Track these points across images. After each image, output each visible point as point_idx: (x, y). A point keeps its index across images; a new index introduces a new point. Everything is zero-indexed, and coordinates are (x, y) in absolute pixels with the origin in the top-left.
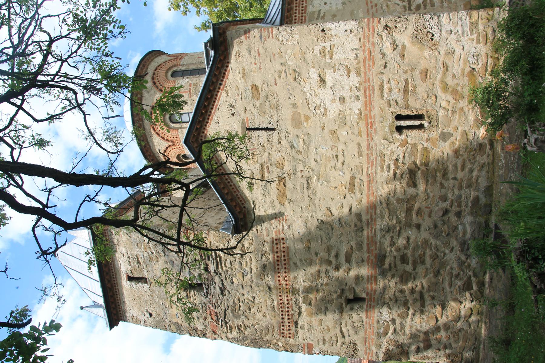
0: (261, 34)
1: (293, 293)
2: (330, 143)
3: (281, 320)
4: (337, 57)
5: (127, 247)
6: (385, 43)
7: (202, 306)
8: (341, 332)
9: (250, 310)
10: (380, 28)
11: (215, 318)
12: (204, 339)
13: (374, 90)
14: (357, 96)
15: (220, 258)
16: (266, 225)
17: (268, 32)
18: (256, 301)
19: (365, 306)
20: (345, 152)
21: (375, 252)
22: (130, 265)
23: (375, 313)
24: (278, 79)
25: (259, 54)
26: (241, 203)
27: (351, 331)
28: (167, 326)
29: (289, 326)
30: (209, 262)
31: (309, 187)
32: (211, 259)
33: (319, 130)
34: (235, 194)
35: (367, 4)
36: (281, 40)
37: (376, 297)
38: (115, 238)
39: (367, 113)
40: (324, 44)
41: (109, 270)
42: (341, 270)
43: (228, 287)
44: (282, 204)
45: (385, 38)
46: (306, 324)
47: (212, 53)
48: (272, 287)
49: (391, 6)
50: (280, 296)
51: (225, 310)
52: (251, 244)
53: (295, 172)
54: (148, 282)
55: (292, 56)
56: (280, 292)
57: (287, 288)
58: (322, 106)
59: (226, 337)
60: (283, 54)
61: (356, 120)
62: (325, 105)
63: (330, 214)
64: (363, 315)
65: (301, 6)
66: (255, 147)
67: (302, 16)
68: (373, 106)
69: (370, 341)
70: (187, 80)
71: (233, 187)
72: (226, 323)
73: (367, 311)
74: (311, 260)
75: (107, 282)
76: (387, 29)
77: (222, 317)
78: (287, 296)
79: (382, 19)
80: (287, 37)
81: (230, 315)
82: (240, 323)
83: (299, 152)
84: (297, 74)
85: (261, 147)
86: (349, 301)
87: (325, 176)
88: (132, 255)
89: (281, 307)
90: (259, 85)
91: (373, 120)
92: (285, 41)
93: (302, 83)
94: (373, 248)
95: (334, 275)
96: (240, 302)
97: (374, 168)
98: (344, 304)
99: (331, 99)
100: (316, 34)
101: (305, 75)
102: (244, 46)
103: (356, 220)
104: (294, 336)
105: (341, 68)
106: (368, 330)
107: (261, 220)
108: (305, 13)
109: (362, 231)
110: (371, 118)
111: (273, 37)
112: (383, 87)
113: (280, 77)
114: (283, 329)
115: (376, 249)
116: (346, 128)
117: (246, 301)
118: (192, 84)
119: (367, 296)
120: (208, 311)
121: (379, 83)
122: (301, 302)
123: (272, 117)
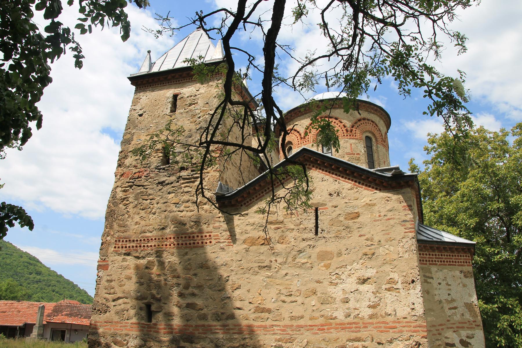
0: (408, 221)
1: (157, 252)
2: (303, 289)
3: (132, 239)
4: (387, 296)
5: (205, 94)
6: (402, 343)
7: (148, 164)
8: (119, 298)
9: (143, 210)
10: (418, 339)
11: (136, 175)
12: (116, 165)
13: (356, 332)
14: (349, 316)
15: (193, 182)
16: (225, 226)
17: (410, 228)
18: (151, 216)
19: (143, 322)
20: (294, 304)
21: (196, 332)
22: (188, 97)
23: (135, 333)
24: (365, 238)
25: (389, 219)
26: (245, 202)
27: (119, 308)
28: (129, 130)
29: (126, 247)
30: (190, 172)
31: (260, 267)
32: (192, 173)
33: (316, 278)
34: (254, 196)
35: (441, 325)
36: (403, 240)
37: (152, 333)
38: (214, 83)
39: (333, 325)
40: (400, 282)
41: (184, 77)
42: (179, 299)
43: (165, 189)
44: (244, 242)
45: (407, 343)
46: (128, 263)
47: (389, 174)
48: (165, 231)
50: (155, 239)
51: (143, 186)
52: (206, 211)
53: (276, 254)
54: (172, 114)
55: (387, 252)
56: (159, 239)
57: (163, 245)
58: (339, 281)
59: (118, 186)
60: (389, 243)
61: (326, 314)
62: (341, 283)
63: (234, 288)
64: (134, 320)
65: (437, 260)
66: (300, 216)
67: (426, 261)
68: (340, 331)
69: (109, 327)
70: (363, 151)
71: (262, 195)
72: (131, 187)
73: (139, 323)
74: (189, 269)
75: (173, 75)
76: (416, 345)
77: (137, 182)
78: (155, 246)
79: (426, 340)
80: (406, 246)
81: (139, 190)
82: (130, 200)
83: (294, 259)
84: (370, 256)
85: (298, 222)
86: (148, 306)
87: (272, 283)
88: (198, 99)
89: (144, 240)
90: (359, 219)
91: (326, 331)
92: (402, 244)
93: (361, 261)
94: (201, 331)
95: (175, 292)
96: (151, 200)
97: (279, 332)
98: (146, 301)
99: (346, 289)
100: (409, 275)
101: (369, 264)
102: (397, 205)
103: (228, 314)
104: (116, 252)
105: (376, 300)
106: (120, 325)
107: (229, 221)
108: (430, 264)
109: (217, 319)
110: (328, 329)
111: (405, 232)
112: (359, 341)
113: (367, 240)
114: (123, 241)
115: (199, 333)
116: (319, 305)
117: (152, 206)
118: (359, 156)
119: (153, 324)
120: (143, 169)
121: (363, 337)
122: (149, 259)
123: (329, 232)
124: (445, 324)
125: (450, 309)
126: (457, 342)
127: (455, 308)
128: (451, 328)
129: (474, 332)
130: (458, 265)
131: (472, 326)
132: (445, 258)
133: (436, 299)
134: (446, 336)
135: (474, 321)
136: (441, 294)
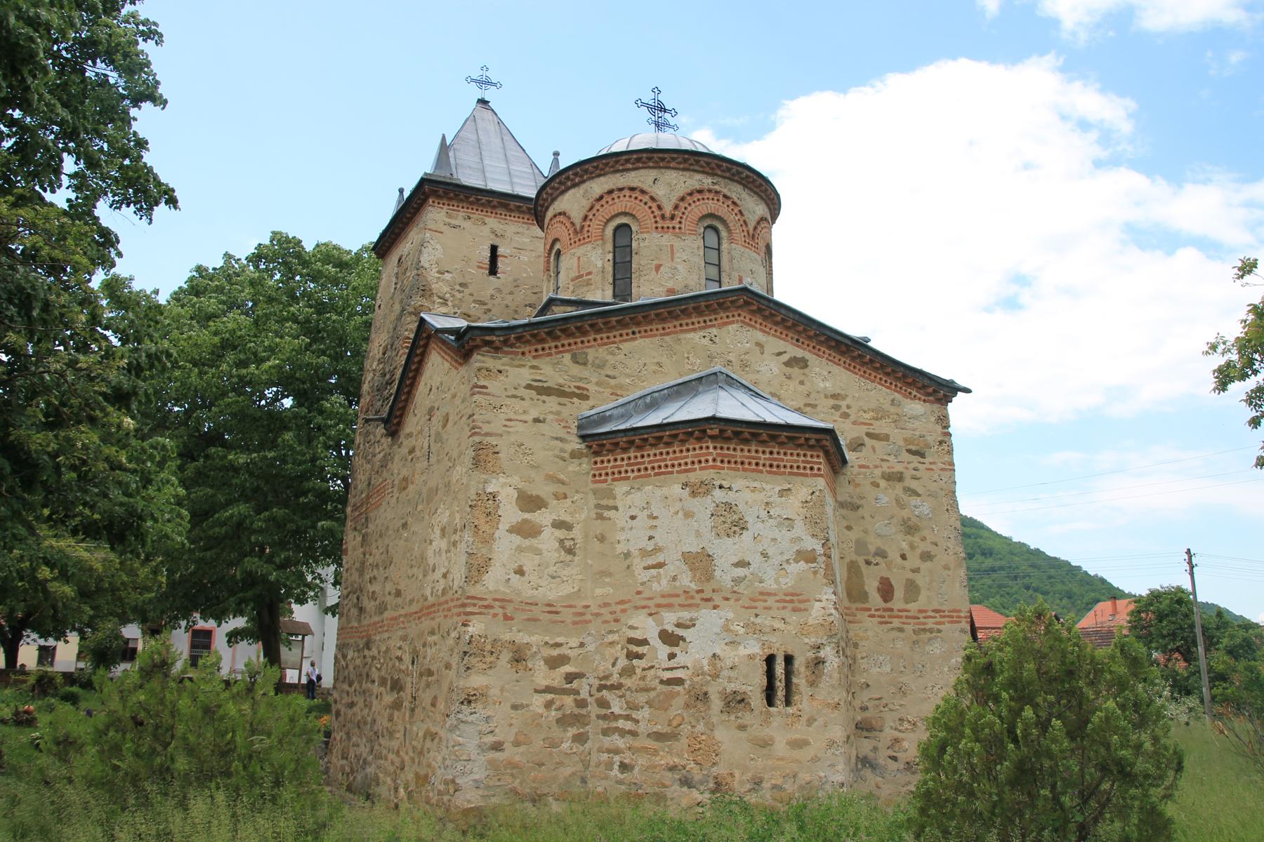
35: (622, 602)
49: (613, 651)
65: (629, 469)
108: (614, 480)
124: (629, 601)
125: (645, 568)
126: (652, 634)
127: (660, 565)
128: (644, 607)
129: (695, 615)
131: (691, 601)
132: (650, 462)
133: (619, 551)
134: (630, 623)
135: (699, 592)
136: (632, 538)
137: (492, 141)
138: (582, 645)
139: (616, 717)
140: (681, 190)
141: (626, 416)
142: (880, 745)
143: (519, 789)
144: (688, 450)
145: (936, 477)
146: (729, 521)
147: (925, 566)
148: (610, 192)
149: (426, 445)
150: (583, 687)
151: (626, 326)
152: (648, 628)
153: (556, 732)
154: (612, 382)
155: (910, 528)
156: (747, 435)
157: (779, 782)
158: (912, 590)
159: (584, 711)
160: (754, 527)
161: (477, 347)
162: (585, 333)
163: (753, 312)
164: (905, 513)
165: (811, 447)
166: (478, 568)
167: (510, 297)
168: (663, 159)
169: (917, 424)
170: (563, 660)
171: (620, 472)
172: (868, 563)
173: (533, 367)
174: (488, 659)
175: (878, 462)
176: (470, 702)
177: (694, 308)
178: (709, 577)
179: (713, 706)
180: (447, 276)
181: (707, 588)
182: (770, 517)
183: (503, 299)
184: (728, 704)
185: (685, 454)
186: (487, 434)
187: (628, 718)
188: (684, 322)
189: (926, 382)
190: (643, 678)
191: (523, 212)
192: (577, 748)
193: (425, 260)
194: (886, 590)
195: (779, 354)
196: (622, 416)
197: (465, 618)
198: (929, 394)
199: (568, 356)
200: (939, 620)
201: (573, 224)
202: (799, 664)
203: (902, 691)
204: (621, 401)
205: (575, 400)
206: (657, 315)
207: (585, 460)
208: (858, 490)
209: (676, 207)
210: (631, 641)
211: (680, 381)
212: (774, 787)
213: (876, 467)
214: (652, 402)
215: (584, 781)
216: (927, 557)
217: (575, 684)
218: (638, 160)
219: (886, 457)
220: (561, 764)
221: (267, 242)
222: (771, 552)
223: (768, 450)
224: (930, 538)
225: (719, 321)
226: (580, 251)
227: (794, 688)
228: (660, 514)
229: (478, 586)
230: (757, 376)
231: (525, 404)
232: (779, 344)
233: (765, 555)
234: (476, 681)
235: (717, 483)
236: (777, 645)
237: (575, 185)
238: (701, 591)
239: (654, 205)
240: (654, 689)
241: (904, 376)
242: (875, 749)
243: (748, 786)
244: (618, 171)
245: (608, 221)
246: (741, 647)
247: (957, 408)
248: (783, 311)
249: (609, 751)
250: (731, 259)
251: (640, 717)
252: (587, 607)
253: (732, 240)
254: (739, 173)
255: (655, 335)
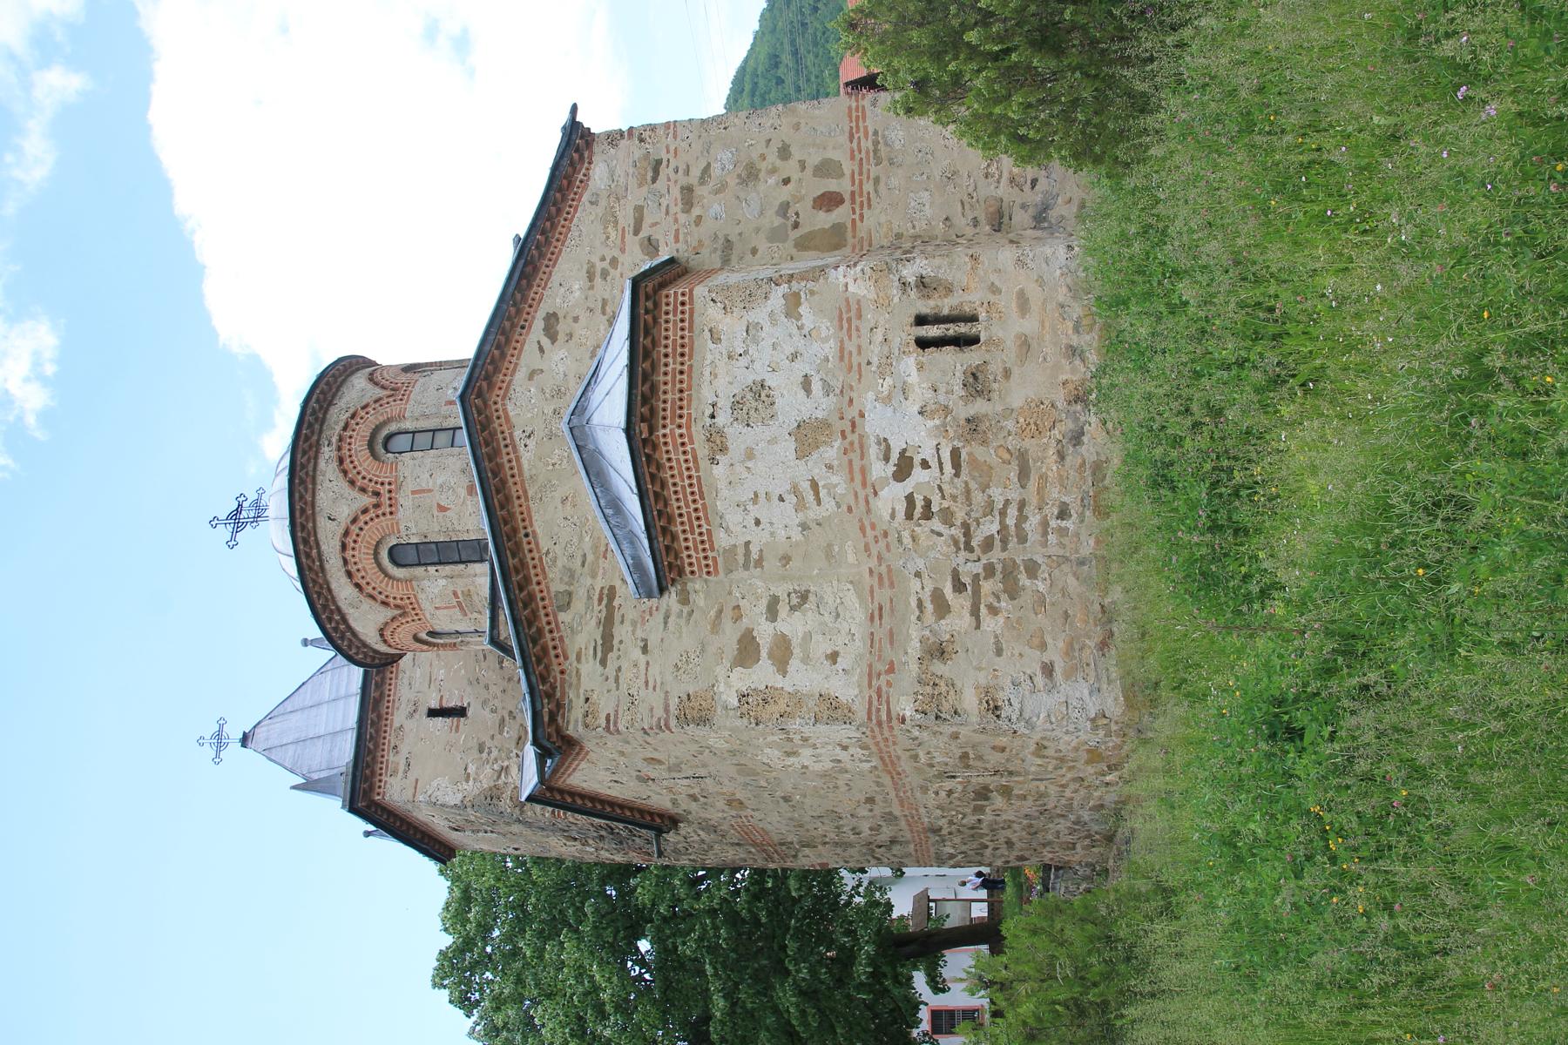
49: (923, 538)
67: (706, 558)
108: (712, 549)
124: (861, 520)
125: (819, 503)
126: (899, 490)
127: (814, 485)
128: (867, 502)
130: (697, 470)
131: (856, 445)
132: (687, 506)
136: (783, 521)
137: (294, 725)
138: (918, 575)
139: (1004, 528)
140: (340, 484)
141: (632, 538)
142: (1019, 201)
143: (1098, 639)
144: (669, 460)
145: (684, 145)
146: (754, 404)
147: (797, 154)
148: (349, 574)
149: (686, 782)
150: (969, 570)
151: (518, 545)
152: (892, 496)
153: (1026, 599)
154: (590, 558)
155: (750, 175)
156: (646, 388)
157: (1070, 324)
158: (826, 169)
159: (999, 567)
160: (760, 372)
161: (558, 731)
162: (531, 597)
163: (491, 386)
164: (732, 182)
165: (656, 305)
166: (832, 709)
167: (493, 689)
168: (303, 511)
169: (619, 171)
170: (938, 596)
171: (702, 542)
172: (796, 225)
173: (578, 659)
174: (943, 689)
175: (670, 219)
176: (996, 708)
177: (490, 461)
178: (824, 425)
179: (983, 411)
180: (472, 769)
181: (839, 425)
182: (746, 352)
183: (495, 697)
184: (980, 393)
185: (674, 464)
186: (667, 710)
187: (1003, 513)
188: (509, 473)
189: (566, 162)
190: (954, 498)
191: (383, 679)
192: (1043, 572)
193: (453, 799)
194: (829, 201)
195: (541, 350)
196: (632, 543)
197: (895, 722)
198: (582, 158)
199: (562, 616)
200: (861, 134)
201: (393, 619)
202: (925, 308)
203: (951, 176)
204: (613, 546)
205: (616, 603)
206: (502, 508)
207: (690, 586)
208: (707, 242)
209: (363, 490)
210: (909, 515)
211: (583, 472)
212: (1076, 330)
213: (676, 220)
214: (611, 507)
215: (1082, 563)
216: (784, 153)
217: (966, 580)
218: (306, 542)
219: (663, 208)
220: (1064, 591)
221: (446, 992)
222: (789, 350)
223: (663, 360)
224: (761, 148)
225: (505, 428)
226: (426, 605)
227: (955, 313)
228: (751, 489)
229: (854, 708)
230: (571, 375)
231: (625, 666)
232: (530, 351)
233: (794, 357)
234: (970, 701)
235: (708, 421)
236: (904, 335)
237: (344, 620)
238: (843, 432)
239: (363, 518)
240: (966, 483)
241: (560, 190)
242: (1024, 206)
243: (1077, 362)
244: (322, 567)
245: (387, 575)
246: (909, 380)
247: (595, 122)
248: (487, 348)
249: (1045, 534)
250: (426, 416)
251: (1002, 499)
252: (871, 571)
253: (401, 417)
254: (314, 412)
255: (528, 508)
